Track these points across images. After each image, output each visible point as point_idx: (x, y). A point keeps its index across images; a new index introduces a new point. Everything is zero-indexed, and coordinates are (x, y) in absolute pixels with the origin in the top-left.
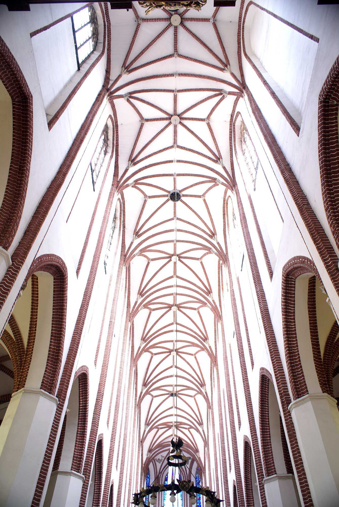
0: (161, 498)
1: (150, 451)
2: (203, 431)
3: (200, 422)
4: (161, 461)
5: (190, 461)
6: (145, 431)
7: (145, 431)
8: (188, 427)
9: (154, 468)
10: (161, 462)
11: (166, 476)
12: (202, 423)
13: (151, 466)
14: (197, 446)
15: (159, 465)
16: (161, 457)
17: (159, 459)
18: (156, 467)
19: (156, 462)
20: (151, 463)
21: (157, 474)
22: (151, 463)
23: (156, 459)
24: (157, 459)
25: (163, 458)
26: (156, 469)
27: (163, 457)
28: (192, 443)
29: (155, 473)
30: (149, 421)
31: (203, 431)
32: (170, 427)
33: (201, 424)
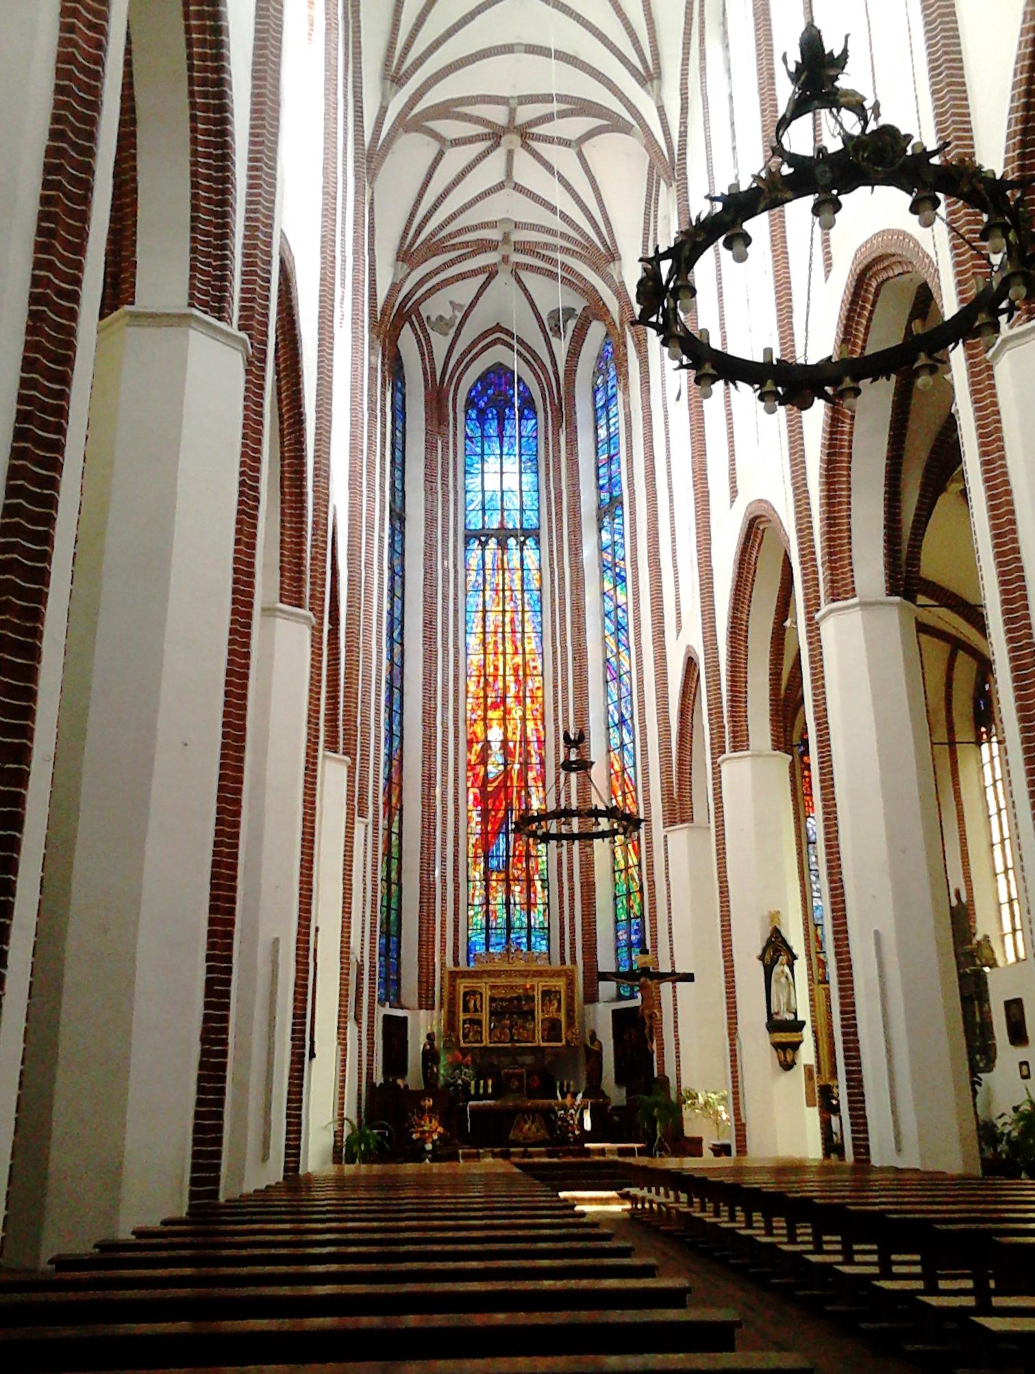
0: (455, 469)
1: (406, 256)
2: (661, 110)
3: (646, 67)
4: (449, 325)
5: (571, 324)
6: (383, 111)
7: (383, 111)
8: (575, 127)
9: (422, 354)
10: (452, 332)
11: (470, 391)
12: (658, 65)
13: (407, 341)
14: (611, 232)
15: (440, 344)
16: (450, 308)
17: (441, 318)
18: (431, 352)
19: (429, 331)
20: (407, 325)
21: (434, 380)
22: (407, 325)
23: (428, 318)
24: (433, 319)
25: (460, 315)
26: (432, 360)
27: (461, 306)
28: (591, 219)
29: (425, 374)
30: (398, 69)
31: (661, 110)
32: (495, 136)
33: (649, 77)
